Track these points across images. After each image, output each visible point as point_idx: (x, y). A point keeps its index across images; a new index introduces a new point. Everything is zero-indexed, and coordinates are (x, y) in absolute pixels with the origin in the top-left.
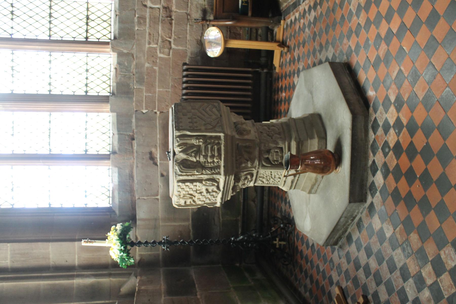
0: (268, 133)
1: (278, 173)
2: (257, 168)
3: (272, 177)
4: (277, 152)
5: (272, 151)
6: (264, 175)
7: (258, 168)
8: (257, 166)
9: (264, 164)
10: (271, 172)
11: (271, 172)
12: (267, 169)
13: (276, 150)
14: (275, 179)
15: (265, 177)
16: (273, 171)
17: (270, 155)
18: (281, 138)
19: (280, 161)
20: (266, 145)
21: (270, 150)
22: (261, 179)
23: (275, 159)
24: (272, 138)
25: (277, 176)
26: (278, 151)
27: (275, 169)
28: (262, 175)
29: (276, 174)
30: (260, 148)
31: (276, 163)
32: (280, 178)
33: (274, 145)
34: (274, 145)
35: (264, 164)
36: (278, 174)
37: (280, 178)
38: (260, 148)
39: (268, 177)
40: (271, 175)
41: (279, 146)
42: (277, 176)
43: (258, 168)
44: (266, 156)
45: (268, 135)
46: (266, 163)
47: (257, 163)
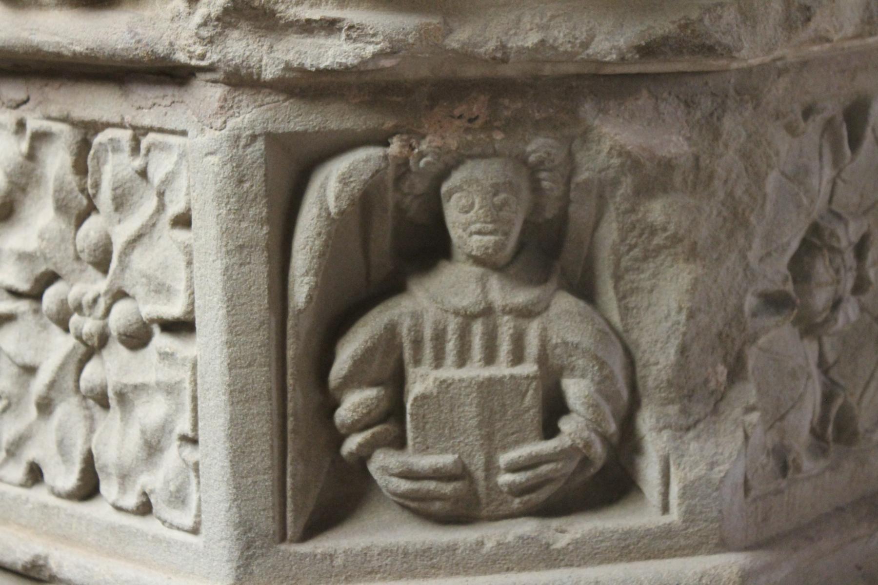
0: (847, 235)
1: (173, 456)
2: (239, 47)
3: (93, 348)
4: (554, 408)
5: (564, 320)
6: (121, 203)
7: (241, 80)
8: (273, 56)
9: (330, 188)
10: (181, 327)
11: (181, 327)
12: (239, 250)
13: (575, 390)
14: (68, 410)
15: (92, 227)
16: (209, 347)
17: (501, 293)
18: (784, 464)
19: (383, 464)
20: (656, 210)
21: (585, 290)
22: (57, 161)
23: (421, 382)
24: (775, 302)
25: (115, 441)
26: (571, 428)
27: (238, 394)
28: (114, 167)
29: (151, 411)
30: (608, 85)
31: (352, 404)
32: (88, 488)
33: (659, 360)
34: (659, 360)
35: (330, 188)
36: (152, 449)
37: (88, 488)
38: (608, 85)
39: (95, 285)
40: (137, 338)
41: (654, 442)
42: (115, 441)
43: (241, 80)
44: (467, 217)
45: (815, 242)
46: (336, 229)
47: (331, 53)
